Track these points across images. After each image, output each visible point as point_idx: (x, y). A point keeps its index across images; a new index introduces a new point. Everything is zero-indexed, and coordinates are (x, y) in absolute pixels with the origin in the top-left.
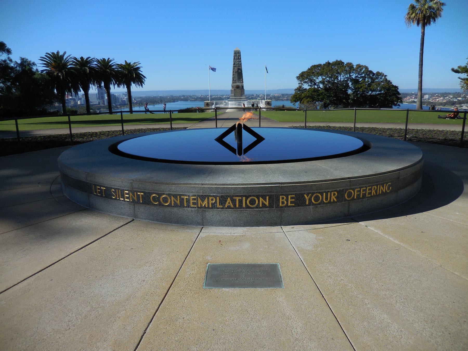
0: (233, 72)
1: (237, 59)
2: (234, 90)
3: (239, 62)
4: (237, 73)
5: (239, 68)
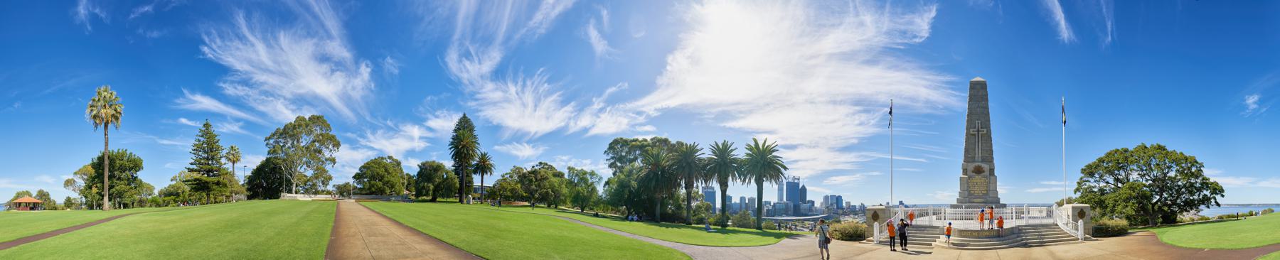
2: (969, 178)
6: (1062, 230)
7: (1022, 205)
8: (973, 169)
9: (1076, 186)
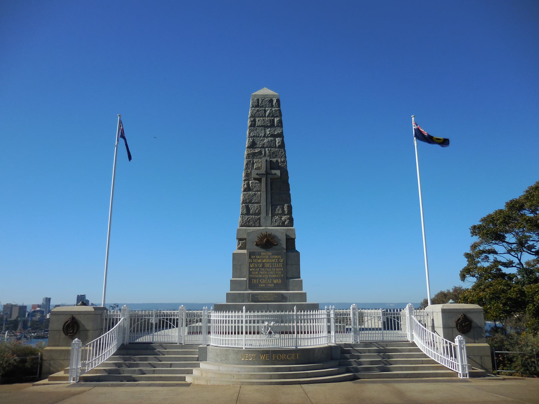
0: (248, 176)
1: (265, 127)
3: (273, 136)
4: (264, 180)
5: (274, 160)
6: (425, 356)
7: (347, 306)
8: (256, 239)
9: (464, 263)
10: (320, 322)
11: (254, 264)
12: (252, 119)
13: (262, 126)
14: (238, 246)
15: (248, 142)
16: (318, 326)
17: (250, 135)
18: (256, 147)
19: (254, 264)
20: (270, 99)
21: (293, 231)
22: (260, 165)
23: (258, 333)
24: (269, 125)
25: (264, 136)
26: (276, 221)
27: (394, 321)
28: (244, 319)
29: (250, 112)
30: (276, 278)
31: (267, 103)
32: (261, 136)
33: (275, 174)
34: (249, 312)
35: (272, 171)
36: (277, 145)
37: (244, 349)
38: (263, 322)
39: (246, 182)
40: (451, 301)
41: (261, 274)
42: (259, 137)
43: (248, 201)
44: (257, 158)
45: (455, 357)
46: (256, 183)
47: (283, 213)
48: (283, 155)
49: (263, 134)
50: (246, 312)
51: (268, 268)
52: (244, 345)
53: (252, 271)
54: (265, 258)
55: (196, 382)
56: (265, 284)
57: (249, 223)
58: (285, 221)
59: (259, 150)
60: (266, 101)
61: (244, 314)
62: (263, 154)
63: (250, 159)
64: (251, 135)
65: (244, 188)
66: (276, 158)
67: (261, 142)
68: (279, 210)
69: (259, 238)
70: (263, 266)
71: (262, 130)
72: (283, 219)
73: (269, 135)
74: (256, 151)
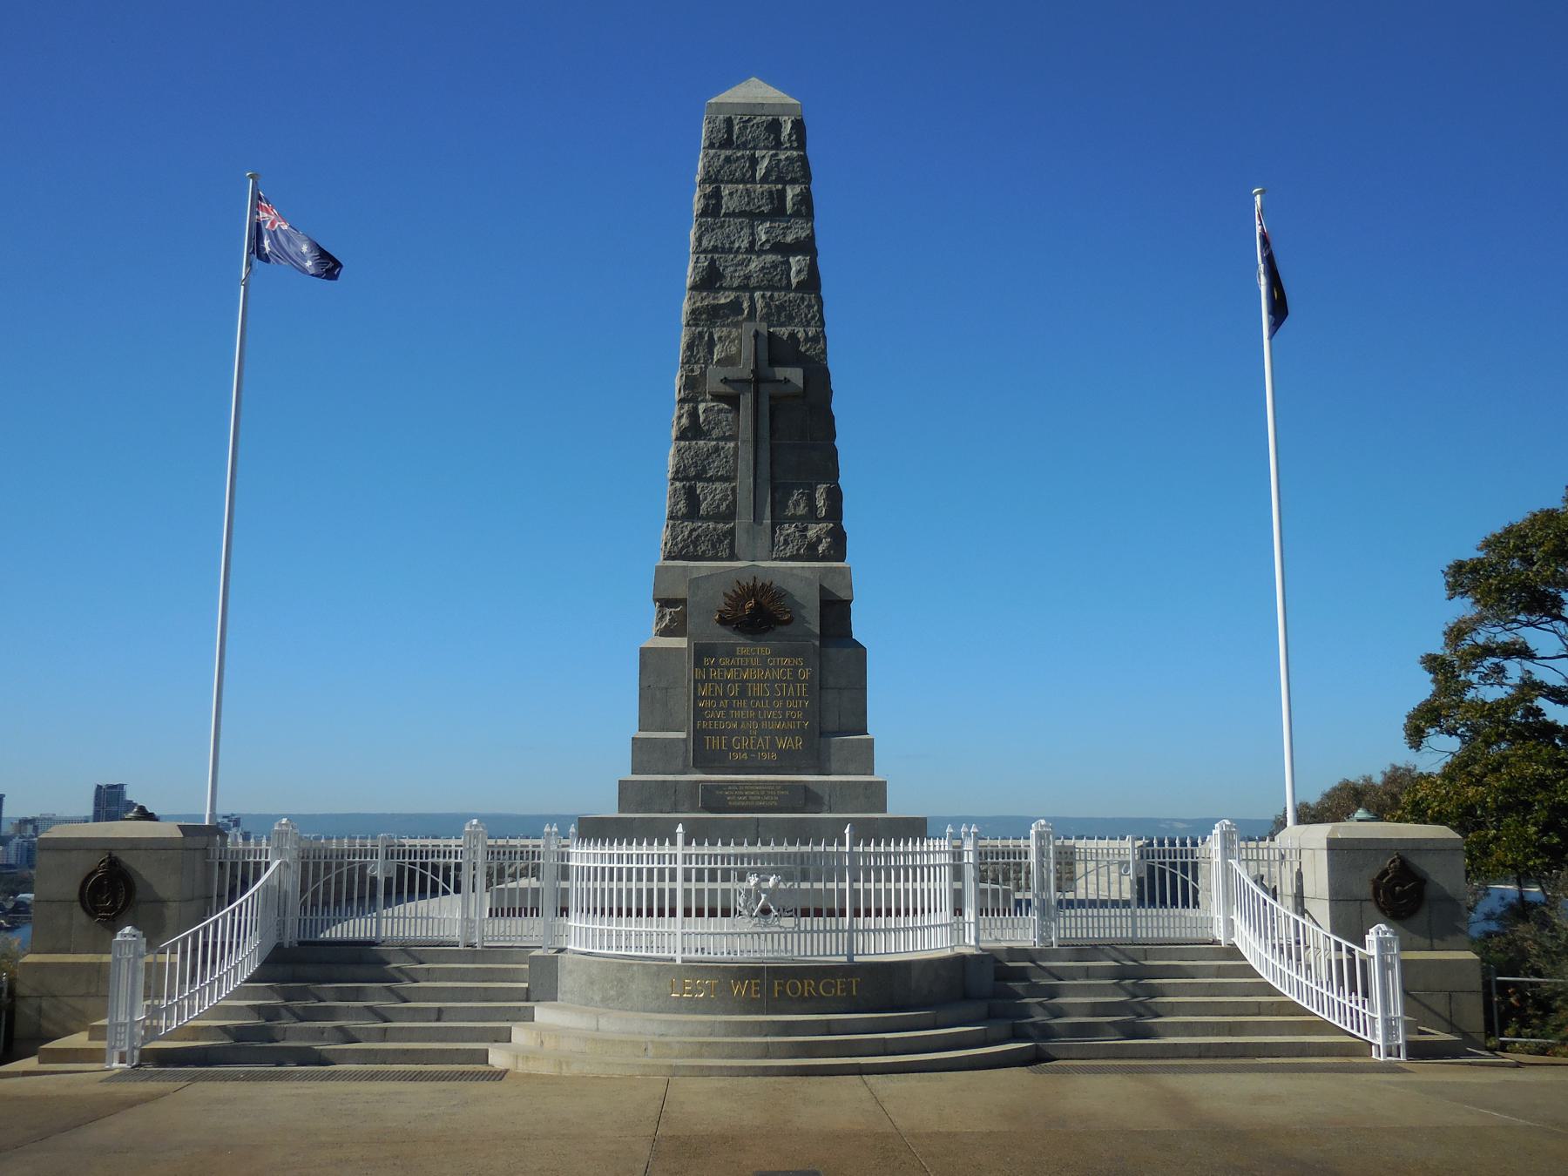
1: (755, 216)
2: (701, 653)
4: (746, 400)
5: (784, 332)
6: (1268, 989)
7: (1020, 827)
10: (929, 880)
11: (713, 687)
12: (709, 188)
13: (742, 214)
14: (657, 624)
15: (695, 268)
16: (922, 891)
17: (700, 244)
18: (721, 288)
19: (713, 687)
20: (770, 118)
21: (845, 574)
22: (734, 349)
23: (726, 913)
24: (766, 209)
25: (750, 249)
26: (786, 543)
27: (1173, 876)
28: (680, 867)
29: (700, 165)
30: (784, 733)
31: (761, 133)
32: (739, 247)
33: (787, 381)
34: (697, 844)
35: (776, 369)
36: (794, 281)
37: (679, 962)
38: (742, 878)
39: (686, 407)
40: (1361, 813)
41: (733, 720)
42: (730, 250)
43: (692, 471)
44: (724, 326)
45: (1366, 994)
46: (720, 411)
47: (812, 515)
48: (813, 317)
49: (746, 242)
50: (687, 843)
51: (760, 698)
52: (679, 949)
53: (703, 709)
54: (750, 666)
55: (523, 1068)
56: (749, 752)
57: (695, 547)
58: (819, 540)
59: (732, 295)
60: (758, 127)
61: (680, 849)
62: (746, 312)
63: (700, 329)
64: (705, 243)
65: (679, 429)
66: (790, 325)
67: (740, 268)
68: (797, 504)
69: (730, 598)
70: (743, 694)
71: (742, 229)
72: (811, 533)
73: (767, 247)
74: (722, 301)
